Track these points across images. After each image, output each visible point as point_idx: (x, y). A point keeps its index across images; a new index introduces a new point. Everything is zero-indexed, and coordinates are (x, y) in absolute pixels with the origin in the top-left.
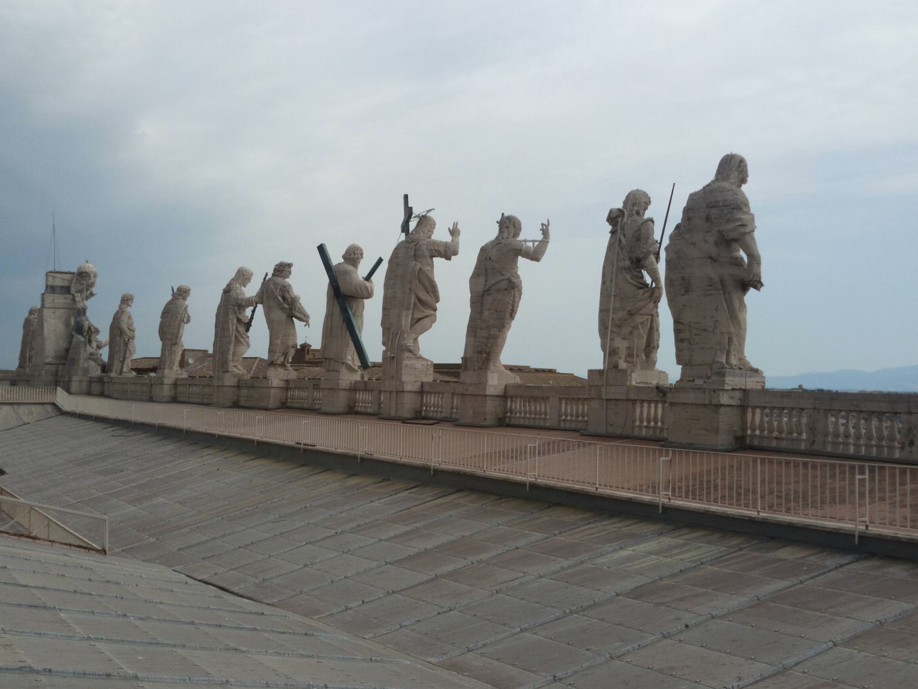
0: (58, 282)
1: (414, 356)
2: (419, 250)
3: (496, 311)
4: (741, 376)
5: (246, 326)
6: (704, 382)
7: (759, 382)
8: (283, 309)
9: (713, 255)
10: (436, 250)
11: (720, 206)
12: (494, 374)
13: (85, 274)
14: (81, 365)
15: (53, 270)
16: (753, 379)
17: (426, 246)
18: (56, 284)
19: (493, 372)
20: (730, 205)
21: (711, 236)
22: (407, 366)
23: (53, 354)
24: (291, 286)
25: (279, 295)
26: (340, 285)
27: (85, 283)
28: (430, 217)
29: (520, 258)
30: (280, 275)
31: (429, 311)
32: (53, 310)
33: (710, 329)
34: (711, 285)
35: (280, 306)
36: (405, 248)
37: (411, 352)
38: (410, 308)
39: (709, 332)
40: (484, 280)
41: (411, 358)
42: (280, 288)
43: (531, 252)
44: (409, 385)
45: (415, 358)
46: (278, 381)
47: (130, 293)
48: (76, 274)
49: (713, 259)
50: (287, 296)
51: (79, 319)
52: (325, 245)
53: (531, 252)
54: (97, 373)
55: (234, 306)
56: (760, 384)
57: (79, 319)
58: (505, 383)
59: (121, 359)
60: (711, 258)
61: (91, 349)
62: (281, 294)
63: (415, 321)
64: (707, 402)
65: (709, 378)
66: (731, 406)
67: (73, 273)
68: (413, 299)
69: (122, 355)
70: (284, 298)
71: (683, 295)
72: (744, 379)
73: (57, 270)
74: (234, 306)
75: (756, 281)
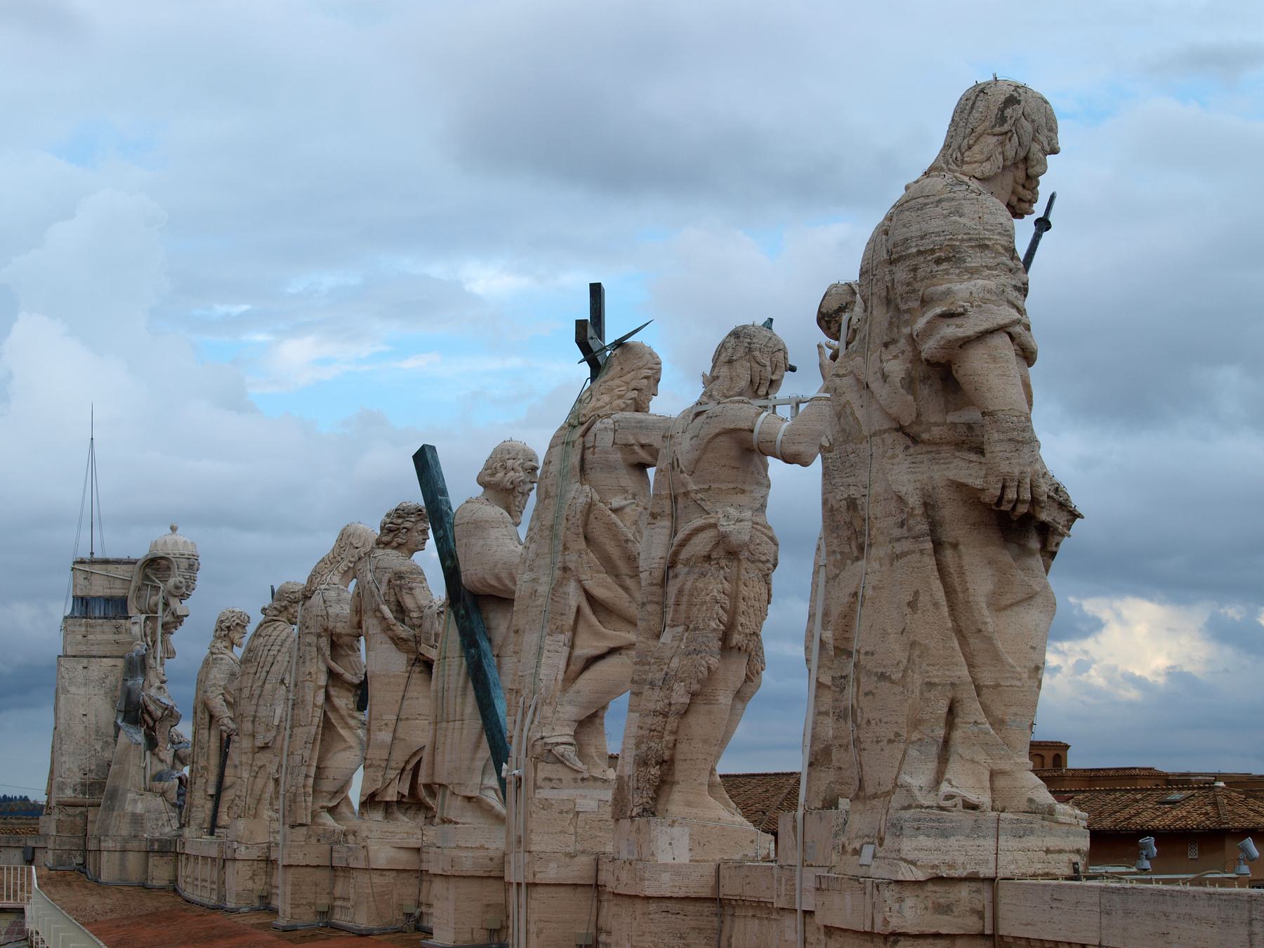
0: (99, 588)
1: (572, 775)
2: (594, 447)
3: (687, 629)
4: (976, 830)
5: (359, 692)
6: (874, 856)
7: (1060, 851)
8: (398, 642)
9: (906, 422)
10: (643, 446)
11: (908, 256)
12: (676, 830)
13: (164, 562)
14: (129, 808)
15: (87, 556)
16: (1032, 842)
17: (611, 434)
18: (93, 593)
19: (672, 825)
20: (933, 251)
21: (896, 357)
22: (546, 805)
23: (78, 778)
24: (421, 573)
25: (387, 602)
26: (462, 568)
27: (161, 585)
28: (642, 346)
29: (770, 459)
30: (394, 544)
31: (622, 634)
32: (85, 662)
33: (896, 676)
34: (902, 525)
35: (389, 632)
36: (563, 443)
37: (562, 762)
38: (119, 633)
39: (892, 682)
40: (667, 531)
41: (560, 780)
42: (390, 581)
43: (780, 437)
44: (553, 865)
45: (575, 780)
46: (393, 853)
47: (237, 610)
48: (139, 563)
49: (909, 434)
50: (409, 602)
51: (129, 683)
52: (433, 448)
53: (780, 437)
54: (167, 829)
55: (319, 636)
56: (1065, 857)
57: (129, 683)
58: (718, 857)
59: (212, 791)
60: (900, 429)
61: (156, 761)
62: (392, 599)
63: (575, 668)
64: (868, 929)
65: (881, 840)
66: (937, 936)
67: (134, 563)
68: (574, 598)
69: (213, 779)
70: (401, 611)
71: (858, 559)
72: (989, 843)
73: (97, 555)
74: (319, 636)
75: (1018, 501)
